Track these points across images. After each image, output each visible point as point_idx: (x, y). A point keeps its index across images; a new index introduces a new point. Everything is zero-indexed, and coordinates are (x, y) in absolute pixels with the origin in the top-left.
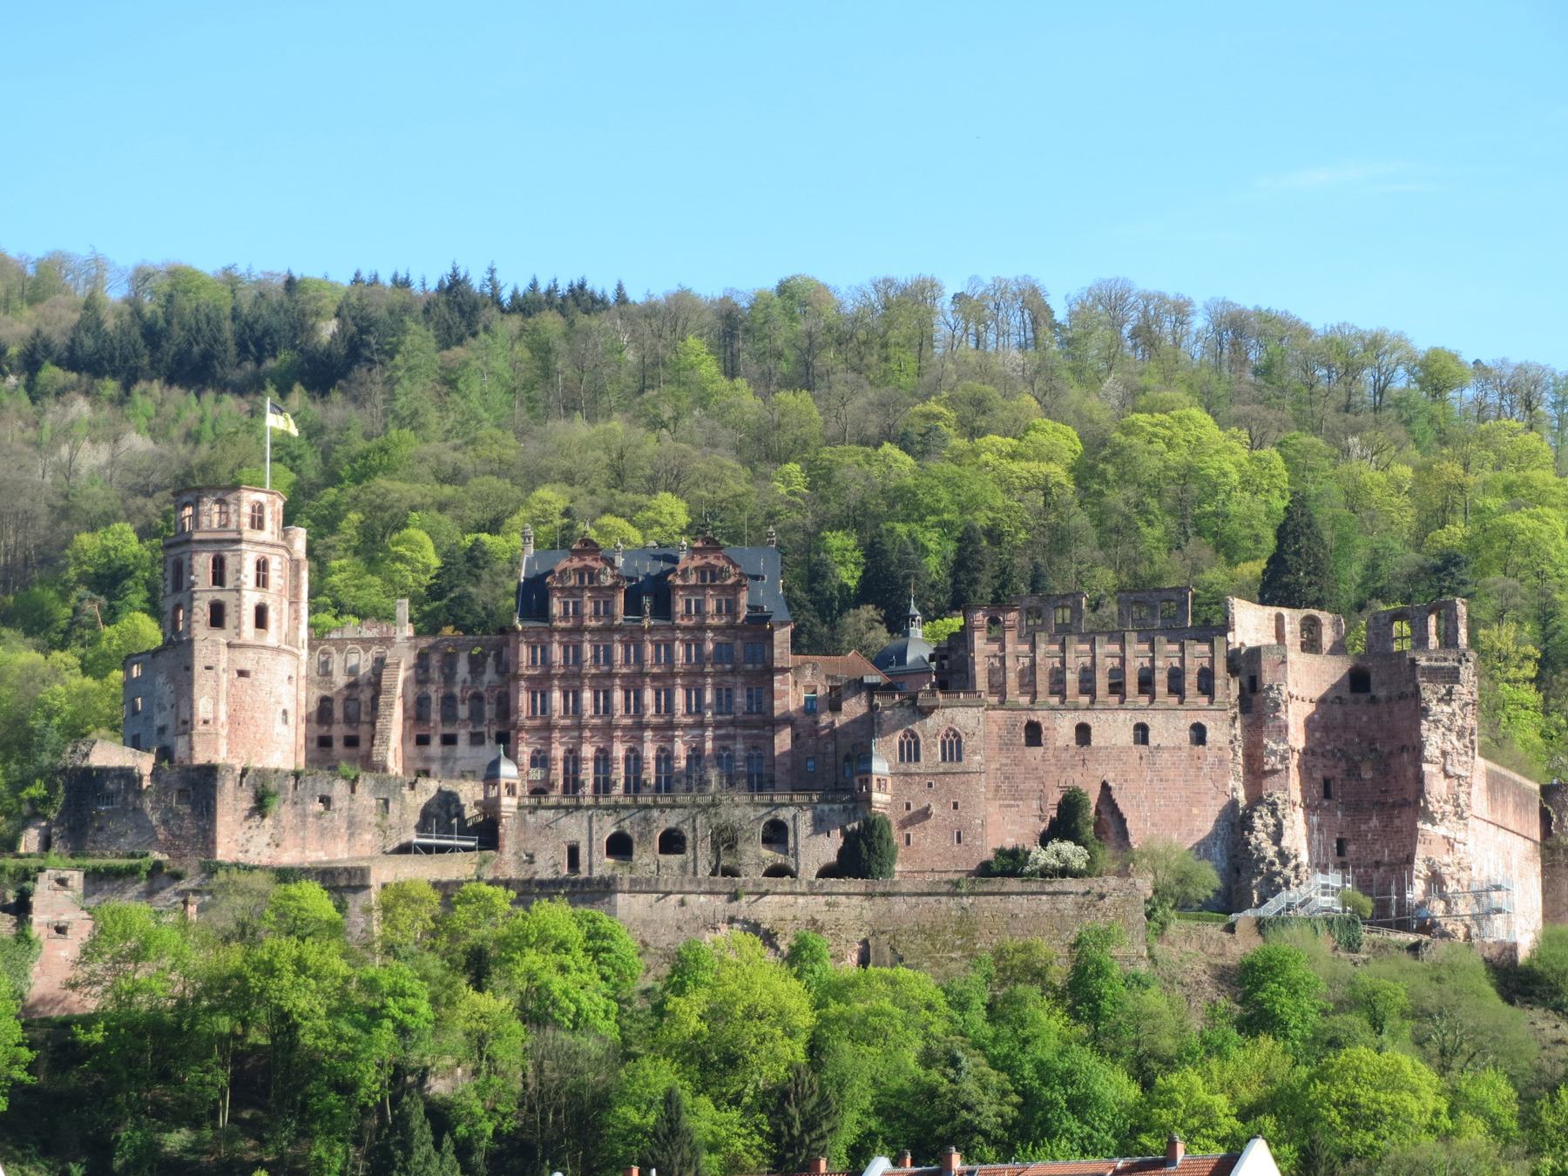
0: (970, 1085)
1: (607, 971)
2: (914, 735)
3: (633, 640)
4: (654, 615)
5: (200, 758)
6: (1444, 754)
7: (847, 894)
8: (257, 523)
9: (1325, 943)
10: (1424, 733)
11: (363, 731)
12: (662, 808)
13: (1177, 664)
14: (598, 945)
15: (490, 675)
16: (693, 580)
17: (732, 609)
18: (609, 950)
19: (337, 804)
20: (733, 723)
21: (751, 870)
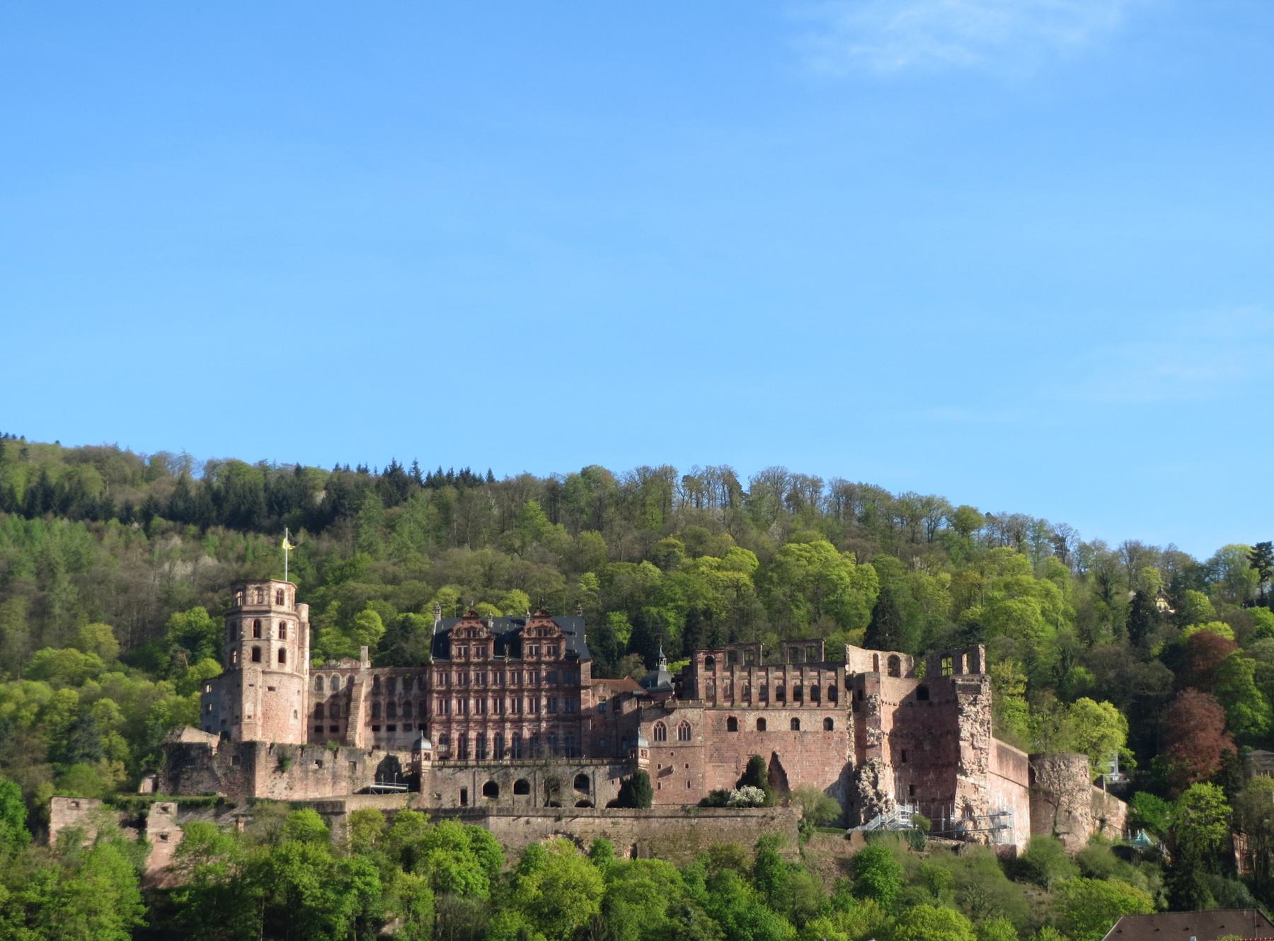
0: (696, 927)
1: (484, 861)
2: (663, 725)
3: (499, 667)
4: (511, 655)
5: (246, 737)
6: (972, 735)
7: (624, 817)
8: (280, 601)
9: (904, 845)
11: (341, 723)
12: (516, 767)
13: (816, 683)
14: (479, 846)
15: (415, 690)
16: (534, 635)
17: (556, 652)
18: (484, 849)
19: (326, 765)
21: (568, 804)
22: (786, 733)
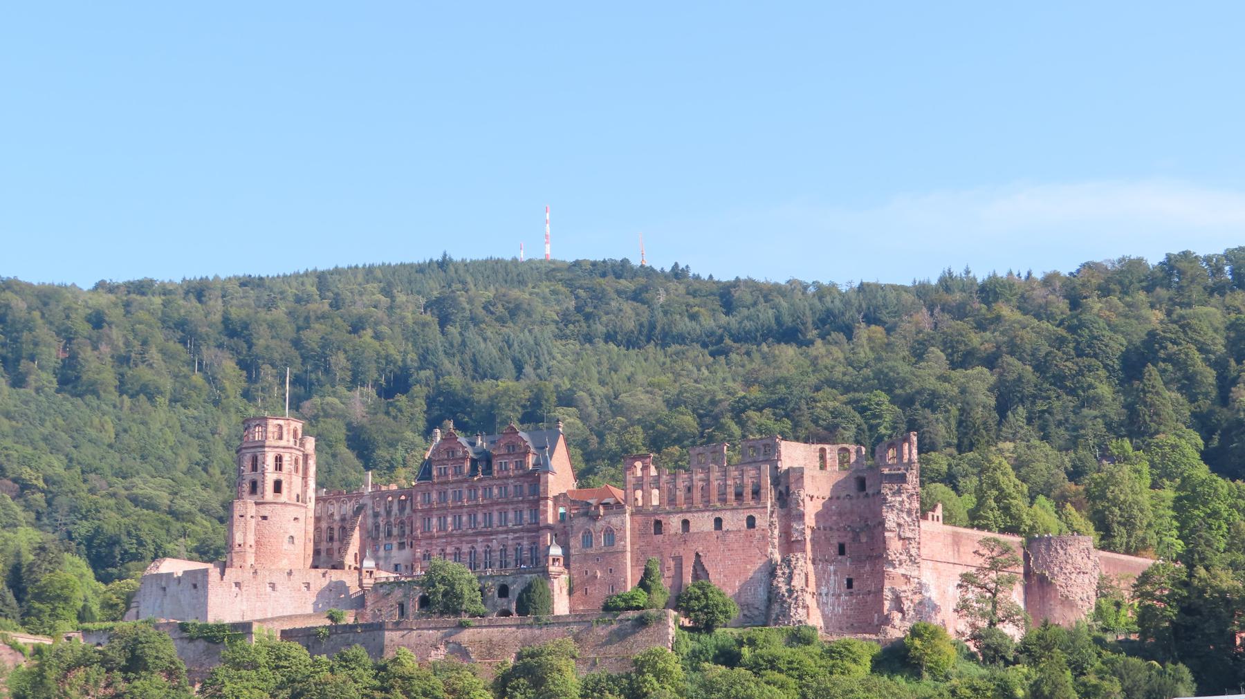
6: (899, 525)
20: (522, 530)
22: (709, 533)
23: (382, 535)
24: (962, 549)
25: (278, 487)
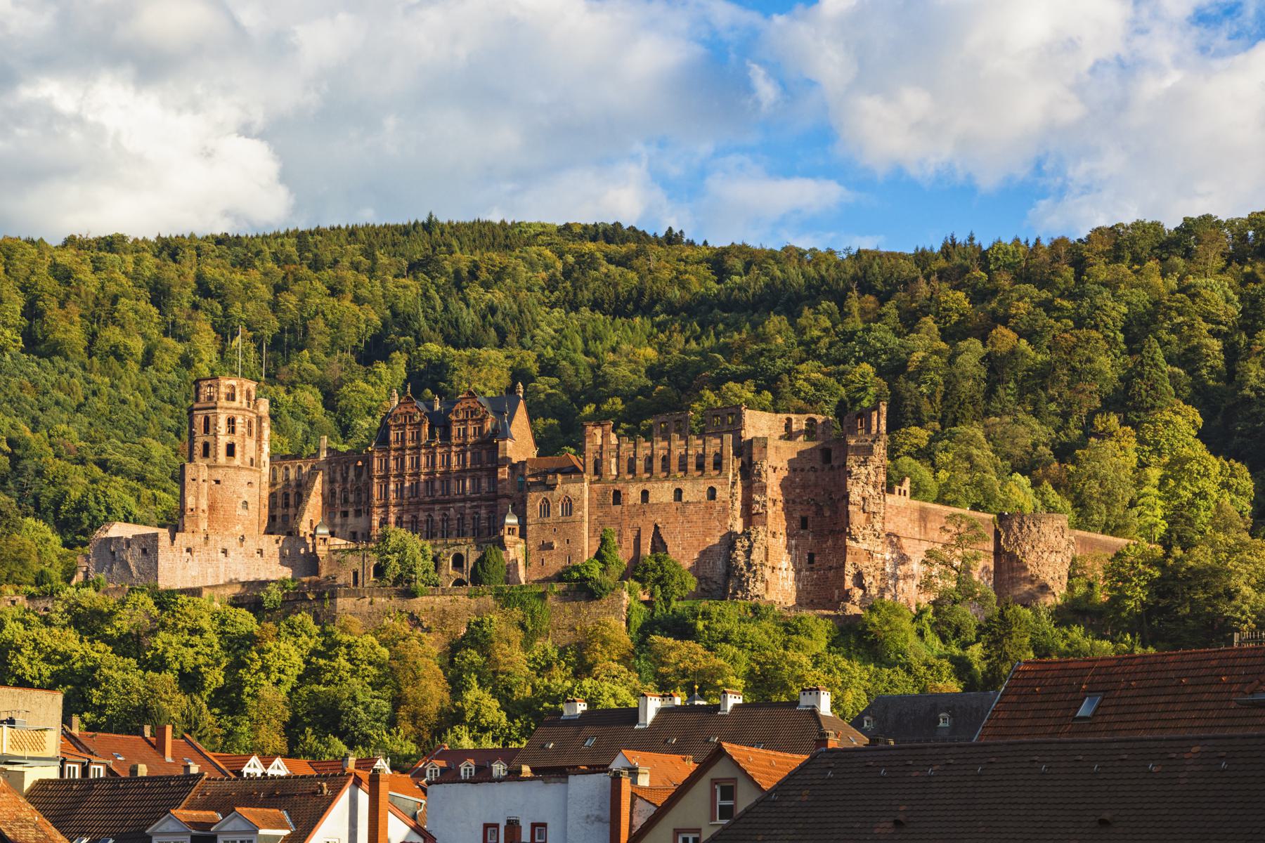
8: (231, 397)
10: (849, 487)
20: (480, 499)
22: (669, 504)
23: (338, 502)
24: (929, 526)
25: (231, 450)
